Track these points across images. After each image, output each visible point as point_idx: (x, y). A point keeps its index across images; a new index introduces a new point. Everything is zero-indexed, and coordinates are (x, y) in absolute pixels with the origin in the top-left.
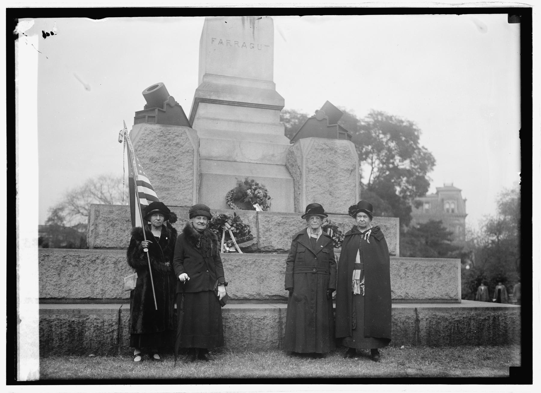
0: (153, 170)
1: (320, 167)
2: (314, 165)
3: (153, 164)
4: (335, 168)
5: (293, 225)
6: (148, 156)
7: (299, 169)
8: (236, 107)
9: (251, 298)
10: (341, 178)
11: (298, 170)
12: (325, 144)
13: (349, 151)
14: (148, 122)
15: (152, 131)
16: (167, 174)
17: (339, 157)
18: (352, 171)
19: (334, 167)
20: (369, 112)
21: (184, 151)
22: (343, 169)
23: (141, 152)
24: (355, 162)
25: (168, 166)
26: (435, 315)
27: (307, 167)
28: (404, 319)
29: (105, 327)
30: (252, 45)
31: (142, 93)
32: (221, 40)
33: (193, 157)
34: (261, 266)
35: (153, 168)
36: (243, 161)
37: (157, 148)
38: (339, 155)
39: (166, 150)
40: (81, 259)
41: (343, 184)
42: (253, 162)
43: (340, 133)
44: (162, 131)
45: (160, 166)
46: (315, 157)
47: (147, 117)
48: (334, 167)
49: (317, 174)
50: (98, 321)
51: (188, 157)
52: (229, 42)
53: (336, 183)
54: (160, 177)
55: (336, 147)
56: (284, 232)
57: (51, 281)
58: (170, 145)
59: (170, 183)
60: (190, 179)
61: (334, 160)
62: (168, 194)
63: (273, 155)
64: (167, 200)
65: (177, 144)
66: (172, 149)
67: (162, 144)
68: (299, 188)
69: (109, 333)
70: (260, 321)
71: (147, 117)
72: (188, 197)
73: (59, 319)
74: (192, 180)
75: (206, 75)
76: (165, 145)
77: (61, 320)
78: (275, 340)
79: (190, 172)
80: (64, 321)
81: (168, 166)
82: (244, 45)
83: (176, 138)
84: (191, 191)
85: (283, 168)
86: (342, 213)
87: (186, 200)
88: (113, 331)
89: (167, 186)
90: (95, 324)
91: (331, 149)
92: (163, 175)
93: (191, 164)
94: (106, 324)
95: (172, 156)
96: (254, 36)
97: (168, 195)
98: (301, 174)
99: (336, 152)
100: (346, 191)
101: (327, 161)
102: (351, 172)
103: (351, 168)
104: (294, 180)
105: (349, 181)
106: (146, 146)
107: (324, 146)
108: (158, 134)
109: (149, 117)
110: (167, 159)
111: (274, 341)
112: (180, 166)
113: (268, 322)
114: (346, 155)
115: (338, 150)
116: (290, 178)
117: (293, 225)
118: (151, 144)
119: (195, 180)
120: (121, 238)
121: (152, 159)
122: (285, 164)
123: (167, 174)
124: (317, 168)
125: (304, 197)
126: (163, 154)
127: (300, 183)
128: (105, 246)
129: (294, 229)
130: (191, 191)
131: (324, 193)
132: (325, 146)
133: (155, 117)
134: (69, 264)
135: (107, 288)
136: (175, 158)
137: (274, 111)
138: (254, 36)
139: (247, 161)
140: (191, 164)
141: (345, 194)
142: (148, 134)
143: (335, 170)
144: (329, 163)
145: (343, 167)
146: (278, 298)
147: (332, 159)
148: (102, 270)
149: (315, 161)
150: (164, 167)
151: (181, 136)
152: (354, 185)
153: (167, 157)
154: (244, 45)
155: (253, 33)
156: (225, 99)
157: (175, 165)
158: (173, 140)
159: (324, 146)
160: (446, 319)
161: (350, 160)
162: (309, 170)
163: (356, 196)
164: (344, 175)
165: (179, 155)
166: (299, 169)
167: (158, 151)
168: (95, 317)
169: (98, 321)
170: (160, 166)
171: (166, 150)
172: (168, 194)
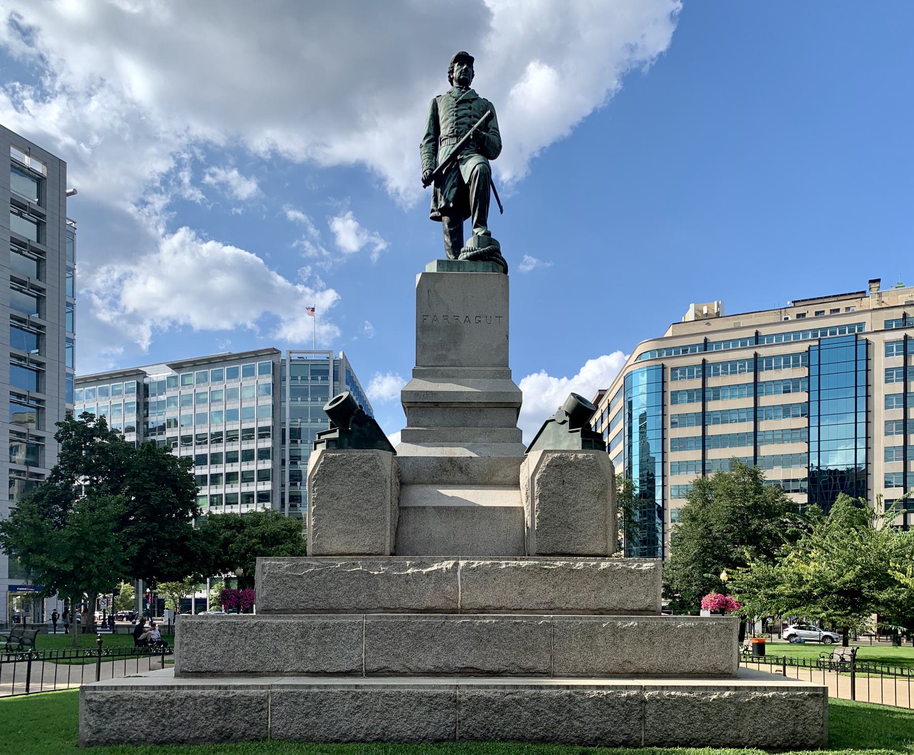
9: (438, 670)
16: (351, 512)
19: (574, 489)
24: (606, 481)
26: (670, 695)
28: (624, 700)
34: (450, 630)
37: (340, 480)
40: (237, 627)
48: (574, 489)
57: (205, 651)
70: (431, 700)
73: (203, 696)
76: (349, 476)
77: (206, 698)
78: (450, 723)
80: (209, 699)
86: (586, 552)
87: (378, 545)
101: (564, 481)
111: (449, 724)
113: (442, 701)
120: (292, 598)
128: (274, 607)
134: (224, 632)
144: (567, 485)
146: (472, 670)
148: (260, 638)
152: (603, 512)
160: (688, 701)
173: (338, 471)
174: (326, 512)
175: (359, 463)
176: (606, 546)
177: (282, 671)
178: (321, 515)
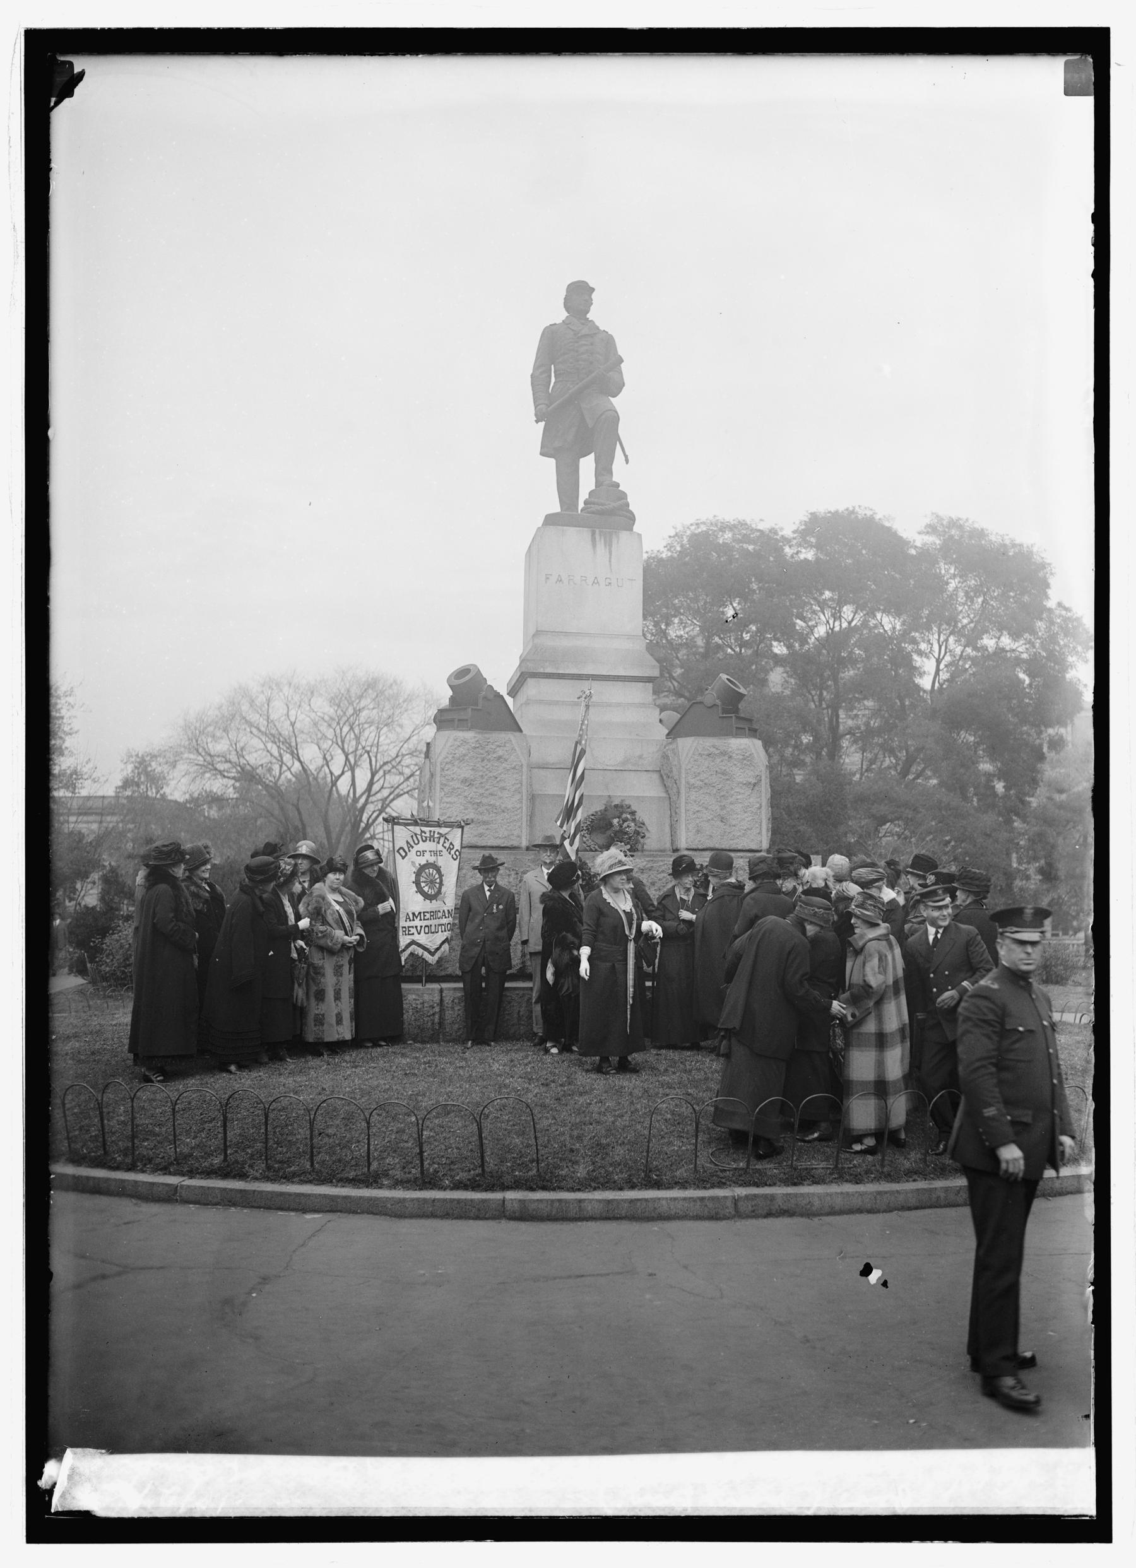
0: (466, 797)
1: (706, 781)
2: (698, 778)
3: (466, 788)
4: (728, 782)
5: (663, 871)
6: (459, 777)
7: (676, 783)
8: (584, 681)
10: (739, 797)
11: (675, 785)
12: (714, 747)
13: (750, 755)
14: (458, 727)
15: (465, 742)
17: (735, 765)
18: (755, 785)
20: (927, 521)
21: (508, 767)
22: (741, 783)
23: (448, 772)
25: (487, 790)
27: (688, 783)
29: (426, 1009)
30: (608, 581)
31: (449, 680)
32: (559, 575)
33: (522, 776)
35: (466, 794)
36: (595, 767)
38: (735, 763)
39: (483, 767)
41: (740, 805)
42: (611, 768)
43: (737, 728)
44: (478, 741)
45: (475, 790)
46: (698, 766)
47: (456, 721)
49: (701, 791)
50: (418, 1002)
51: (515, 776)
52: (572, 578)
53: (731, 803)
54: (475, 806)
55: (730, 750)
56: (650, 881)
58: (489, 760)
59: (489, 814)
60: (518, 806)
61: (728, 770)
62: (487, 829)
63: (640, 757)
64: (486, 838)
65: (500, 758)
66: (493, 765)
67: (479, 759)
68: (676, 813)
69: (429, 1016)
71: (456, 721)
72: (516, 833)
74: (521, 808)
75: (538, 633)
76: (483, 760)
79: (518, 797)
81: (487, 790)
82: (596, 582)
83: (498, 749)
84: (519, 824)
85: (655, 776)
86: (740, 848)
88: (434, 1014)
89: (485, 818)
90: (414, 1005)
91: (723, 753)
92: (480, 802)
93: (519, 785)
94: (426, 1005)
95: (491, 775)
96: (610, 565)
97: (487, 832)
98: (679, 793)
99: (730, 757)
100: (746, 815)
102: (754, 786)
103: (753, 781)
104: (670, 798)
105: (751, 800)
106: (456, 763)
107: (712, 750)
108: (473, 745)
109: (459, 720)
110: (485, 780)
112: (503, 789)
114: (745, 762)
115: (734, 755)
116: (664, 795)
117: (663, 871)
118: (463, 759)
119: (524, 808)
121: (464, 781)
122: (658, 769)
123: (485, 801)
124: (701, 783)
125: (683, 827)
126: (480, 774)
127: (677, 805)
129: (664, 877)
130: (519, 824)
131: (712, 819)
132: (714, 749)
133: (467, 720)
135: (418, 963)
136: (496, 778)
137: (641, 684)
138: (610, 565)
139: (601, 768)
140: (519, 785)
141: (744, 819)
142: (459, 746)
143: (729, 785)
145: (741, 780)
147: (724, 768)
149: (699, 773)
150: (481, 791)
151: (505, 746)
152: (758, 805)
153: (486, 777)
154: (596, 581)
155: (610, 561)
156: (567, 672)
157: (495, 788)
158: (494, 753)
159: (712, 750)
161: (752, 768)
162: (690, 787)
163: (761, 822)
164: (743, 791)
165: (502, 773)
166: (676, 783)
167: (473, 769)
168: (414, 997)
169: (418, 1002)
170: (475, 790)
171: (483, 767)
172: (487, 829)
173: (470, 755)
174: (456, 800)
175: (493, 747)
176: (761, 842)
177: (435, 976)
178: (450, 803)
